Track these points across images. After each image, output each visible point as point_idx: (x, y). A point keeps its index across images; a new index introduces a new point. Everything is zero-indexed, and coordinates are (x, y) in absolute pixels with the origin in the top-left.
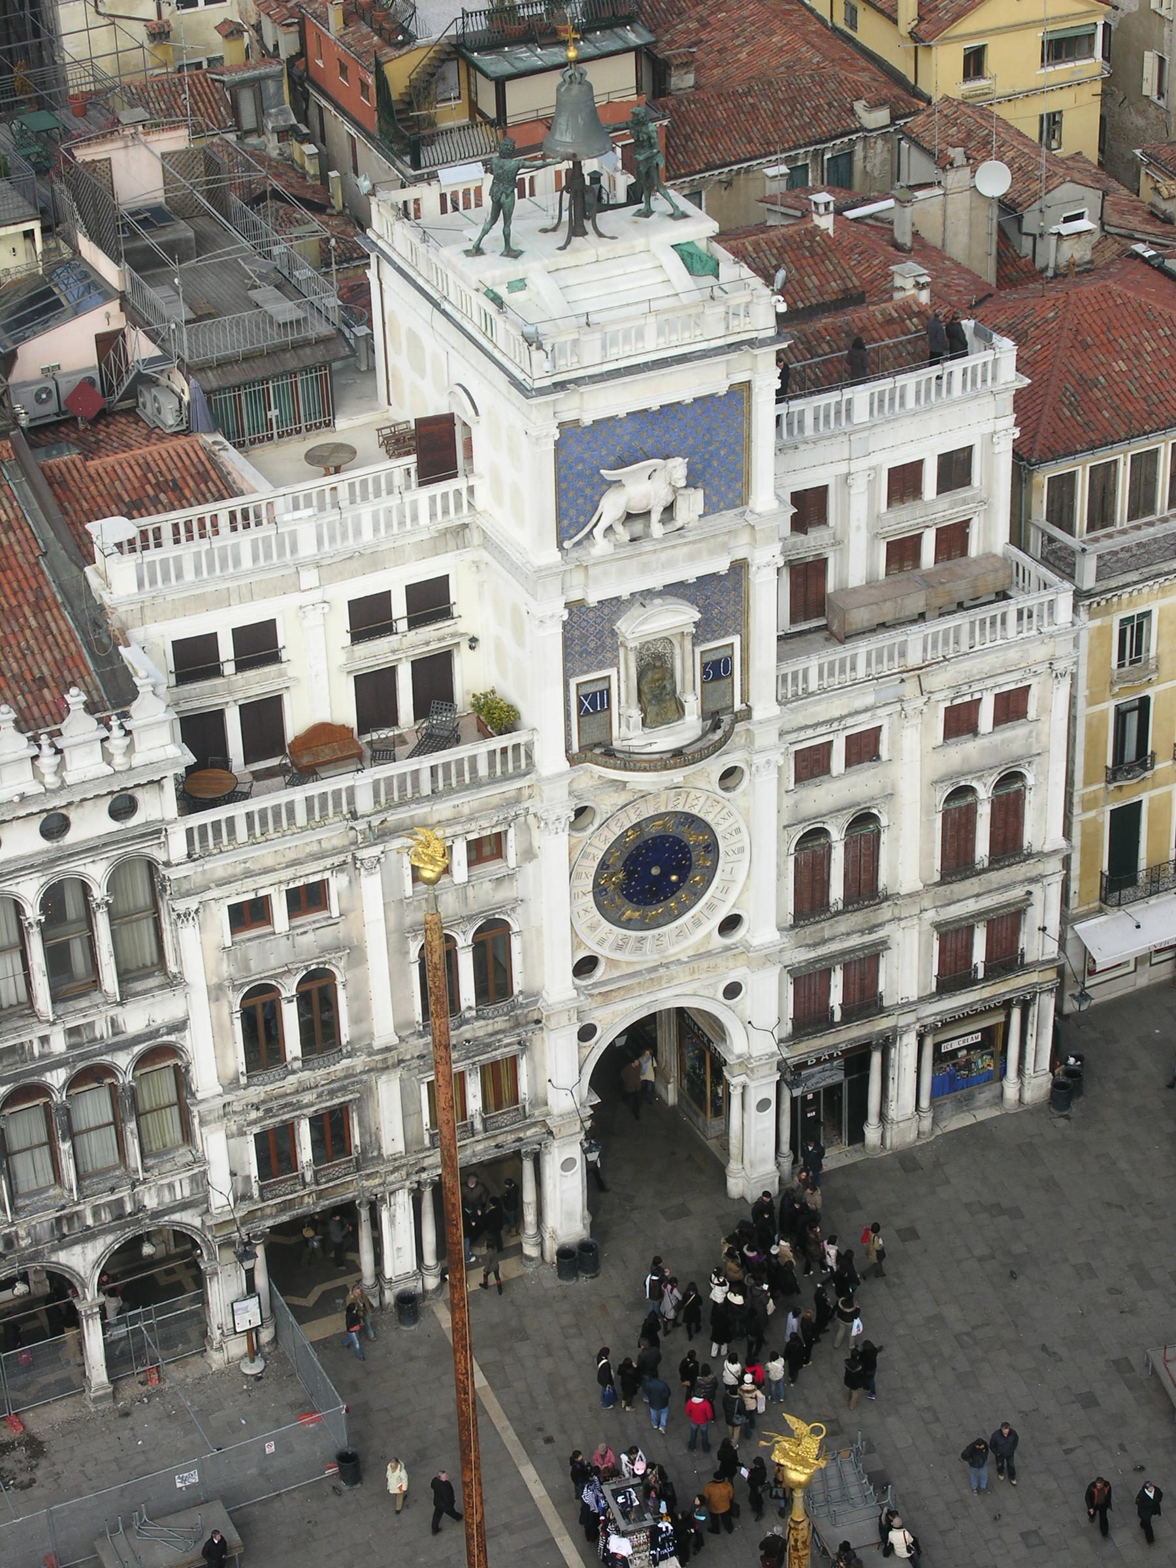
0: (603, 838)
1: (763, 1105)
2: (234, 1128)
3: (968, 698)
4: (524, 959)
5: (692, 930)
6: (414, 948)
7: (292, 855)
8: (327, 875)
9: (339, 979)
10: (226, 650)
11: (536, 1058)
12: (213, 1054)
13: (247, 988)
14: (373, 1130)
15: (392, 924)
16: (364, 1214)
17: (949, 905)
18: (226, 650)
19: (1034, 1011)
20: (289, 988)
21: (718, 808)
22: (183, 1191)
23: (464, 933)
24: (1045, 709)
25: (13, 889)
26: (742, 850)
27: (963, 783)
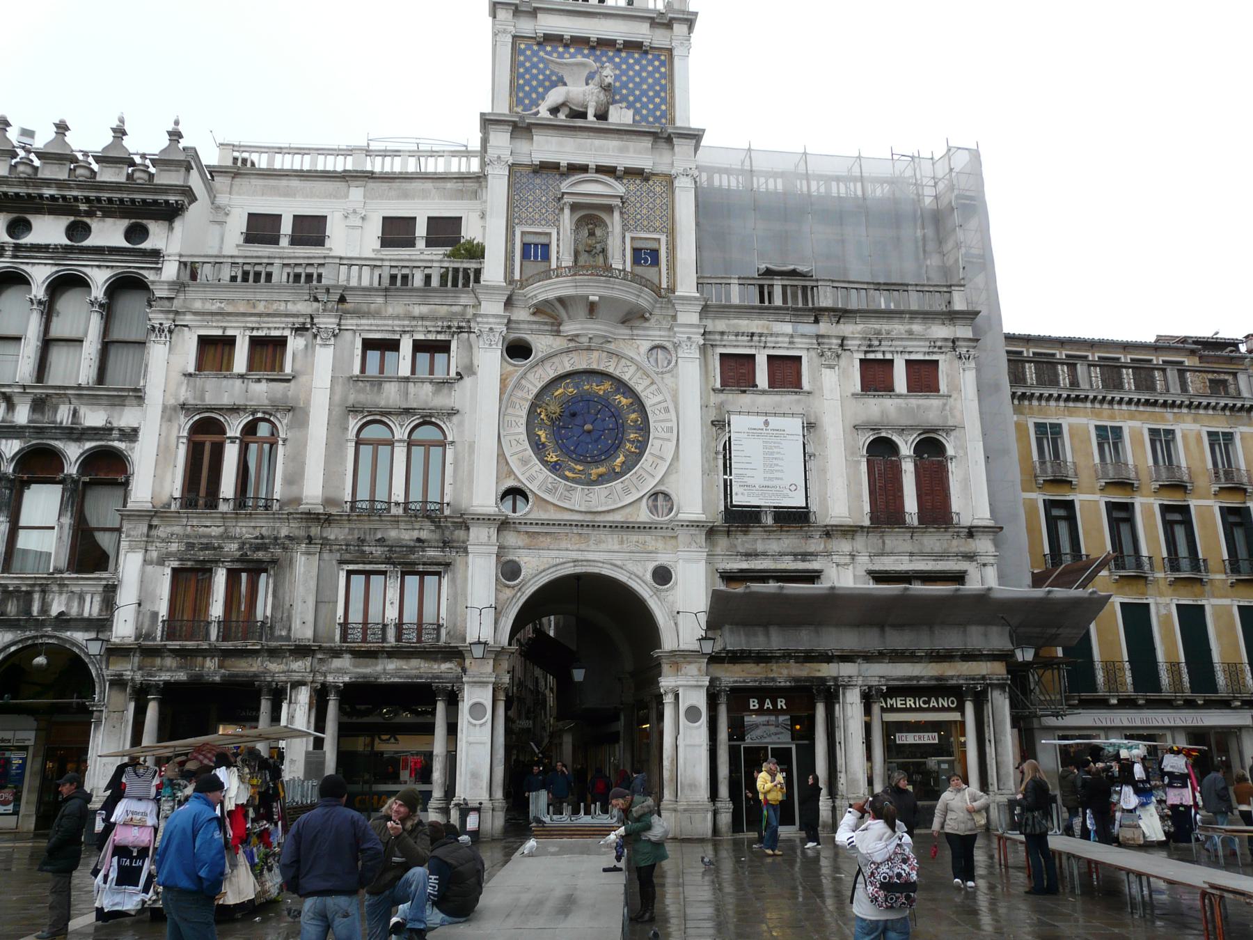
0: (537, 375)
1: (693, 713)
2: (154, 555)
3: (880, 356)
4: (455, 471)
5: (622, 496)
6: (353, 424)
7: (261, 308)
8: (287, 333)
9: (282, 435)
10: (286, 228)
11: (459, 582)
12: (155, 473)
13: (197, 417)
14: (287, 606)
15: (337, 398)
16: (265, 705)
17: (882, 554)
18: (286, 228)
19: (988, 709)
20: (234, 427)
21: (648, 381)
22: (92, 608)
23: (401, 426)
24: (955, 387)
25: (27, 268)
26: (670, 430)
27: (883, 434)
